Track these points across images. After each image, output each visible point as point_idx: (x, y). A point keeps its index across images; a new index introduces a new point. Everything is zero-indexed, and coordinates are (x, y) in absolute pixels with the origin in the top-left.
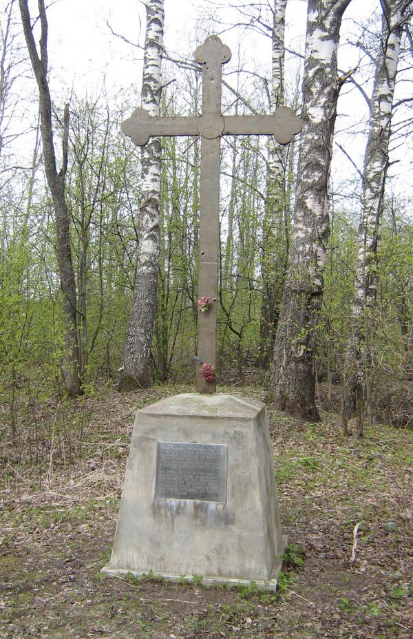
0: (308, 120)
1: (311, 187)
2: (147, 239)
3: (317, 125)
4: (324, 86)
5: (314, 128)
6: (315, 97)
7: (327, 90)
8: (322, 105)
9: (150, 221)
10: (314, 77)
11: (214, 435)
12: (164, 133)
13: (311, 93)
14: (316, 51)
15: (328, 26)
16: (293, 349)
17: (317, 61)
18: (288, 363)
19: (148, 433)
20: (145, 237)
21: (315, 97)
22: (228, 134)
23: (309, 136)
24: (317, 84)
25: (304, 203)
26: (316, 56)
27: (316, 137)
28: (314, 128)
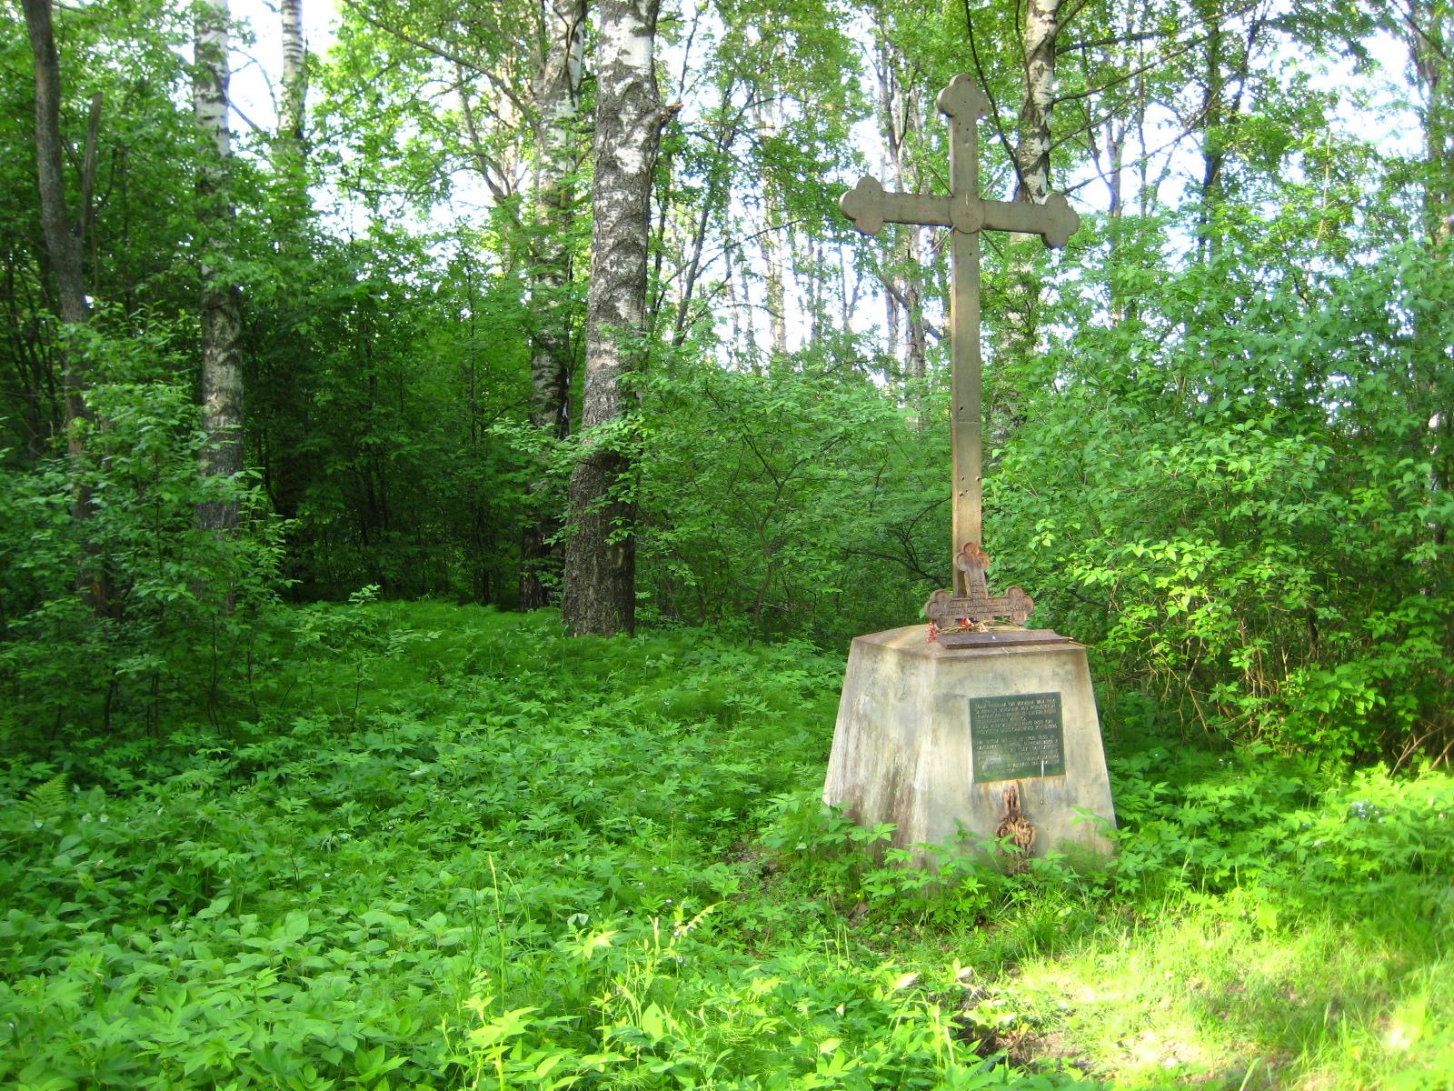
0: (615, 167)
1: (624, 283)
2: (224, 363)
3: (633, 178)
4: (644, 112)
5: (625, 182)
6: (628, 129)
7: (649, 119)
8: (639, 143)
9: (229, 330)
10: (624, 95)
11: (1041, 679)
12: (922, 220)
13: (620, 123)
14: (625, 52)
15: (644, 12)
16: (609, 555)
17: (629, 70)
18: (601, 581)
19: (953, 687)
20: (221, 358)
21: (628, 129)
22: (989, 228)
23: (618, 196)
24: (630, 108)
25: (614, 308)
26: (626, 60)
27: (631, 199)
28: (625, 182)
